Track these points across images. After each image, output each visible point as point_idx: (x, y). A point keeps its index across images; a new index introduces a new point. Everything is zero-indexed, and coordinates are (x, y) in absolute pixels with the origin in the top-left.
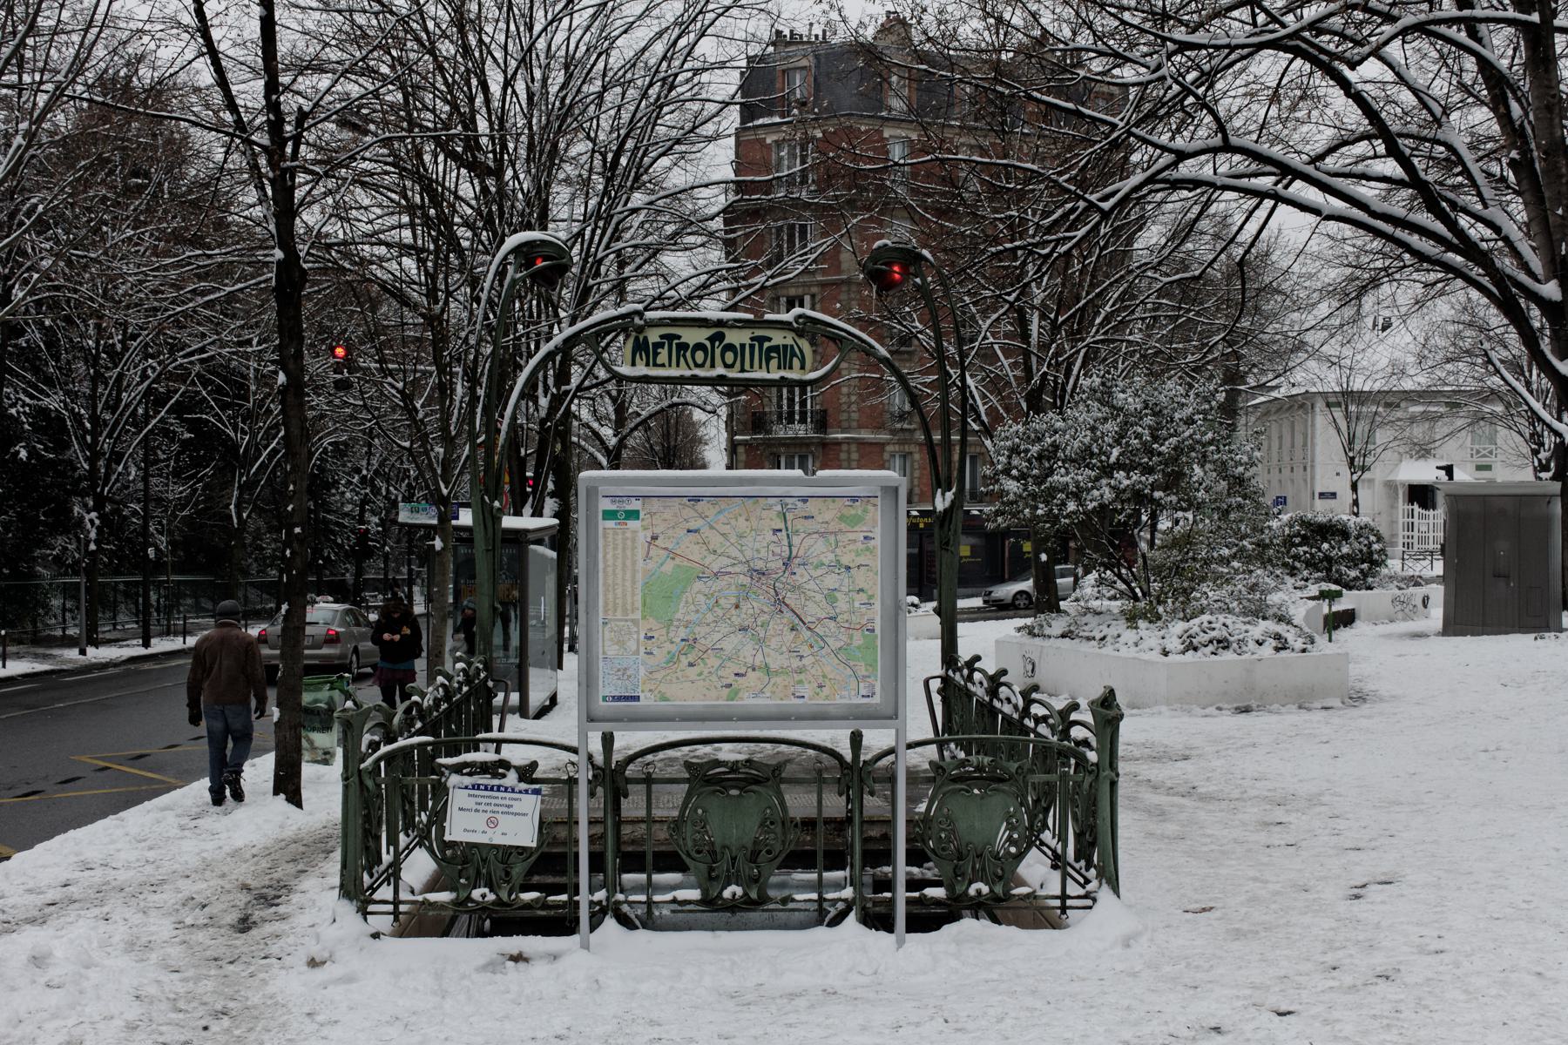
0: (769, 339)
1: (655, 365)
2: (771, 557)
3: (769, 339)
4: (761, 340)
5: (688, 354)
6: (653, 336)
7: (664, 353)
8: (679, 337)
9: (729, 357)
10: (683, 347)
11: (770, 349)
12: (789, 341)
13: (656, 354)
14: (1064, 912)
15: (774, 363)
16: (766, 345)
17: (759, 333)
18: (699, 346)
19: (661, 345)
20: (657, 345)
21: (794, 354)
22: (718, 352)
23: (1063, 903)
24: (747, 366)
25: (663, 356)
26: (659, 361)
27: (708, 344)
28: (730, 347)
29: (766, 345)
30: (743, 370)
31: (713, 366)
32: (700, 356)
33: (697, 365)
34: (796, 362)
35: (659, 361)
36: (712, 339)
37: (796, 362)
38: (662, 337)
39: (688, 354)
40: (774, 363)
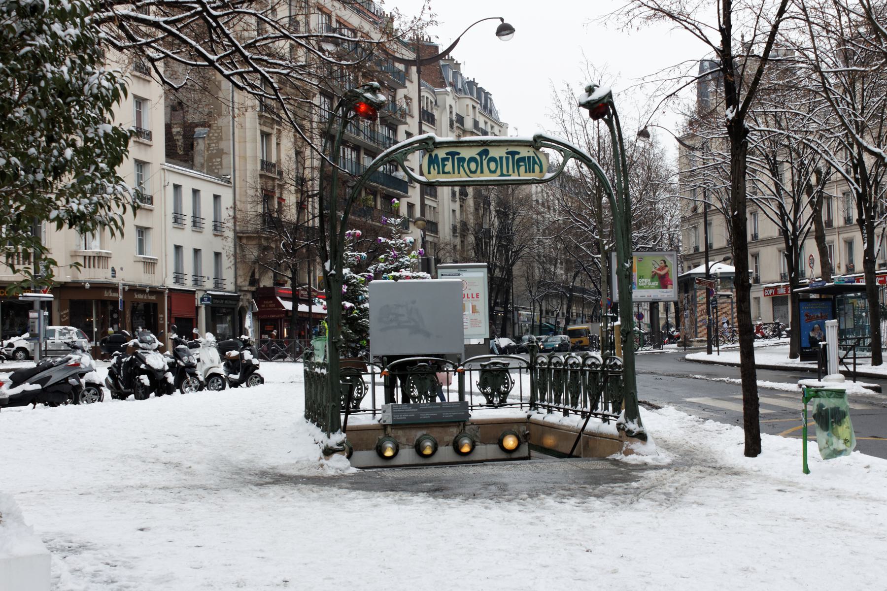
0: (518, 153)
1: (444, 173)
3: (518, 153)
4: (513, 154)
5: (465, 165)
7: (449, 164)
8: (459, 154)
9: (493, 165)
10: (462, 160)
12: (531, 154)
13: (444, 166)
15: (522, 169)
16: (517, 157)
17: (511, 149)
18: (472, 159)
19: (447, 159)
20: (444, 160)
21: (535, 163)
22: (485, 163)
24: (505, 172)
25: (449, 167)
26: (446, 170)
27: (478, 158)
28: (493, 159)
29: (517, 157)
30: (502, 175)
31: (482, 172)
32: (473, 166)
33: (471, 172)
34: (537, 168)
35: (446, 170)
36: (480, 154)
37: (537, 168)
38: (447, 154)
40: (522, 169)
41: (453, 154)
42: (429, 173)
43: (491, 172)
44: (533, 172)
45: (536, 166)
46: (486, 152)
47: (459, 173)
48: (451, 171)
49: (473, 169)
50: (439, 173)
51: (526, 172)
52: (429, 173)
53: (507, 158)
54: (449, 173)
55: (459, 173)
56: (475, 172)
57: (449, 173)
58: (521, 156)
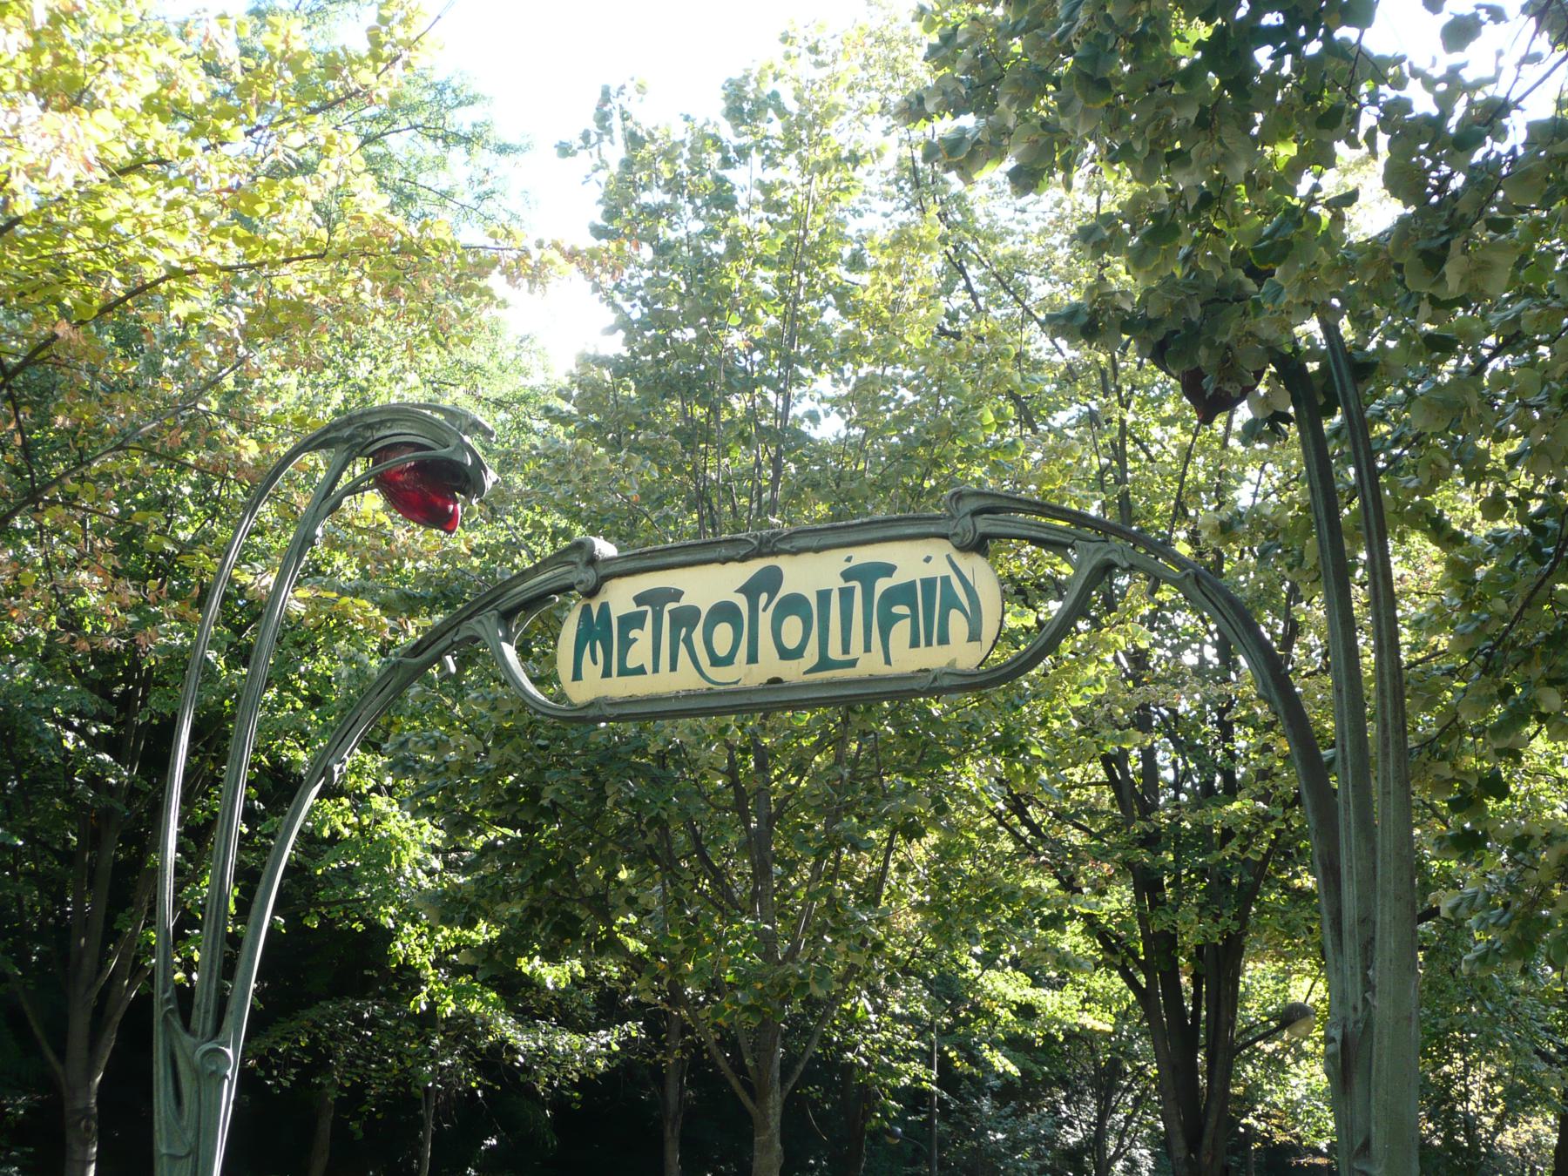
1: (624, 672)
3: (888, 570)
4: (867, 574)
5: (698, 636)
7: (642, 638)
8: (677, 595)
9: (792, 629)
10: (685, 618)
11: (891, 596)
13: (626, 644)
16: (882, 585)
18: (725, 612)
20: (631, 621)
21: (951, 602)
22: (765, 619)
24: (835, 652)
25: (640, 654)
27: (742, 602)
28: (795, 604)
29: (882, 585)
31: (752, 658)
32: (723, 635)
33: (716, 661)
34: (958, 624)
35: (631, 663)
36: (750, 590)
37: (958, 624)
38: (640, 599)
39: (698, 636)
42: (577, 676)
43: (785, 654)
44: (944, 640)
46: (771, 580)
47: (673, 668)
48: (649, 667)
49: (722, 650)
50: (607, 673)
51: (915, 643)
52: (577, 676)
53: (846, 595)
54: (640, 671)
55: (673, 668)
56: (728, 660)
57: (640, 671)
58: (897, 579)
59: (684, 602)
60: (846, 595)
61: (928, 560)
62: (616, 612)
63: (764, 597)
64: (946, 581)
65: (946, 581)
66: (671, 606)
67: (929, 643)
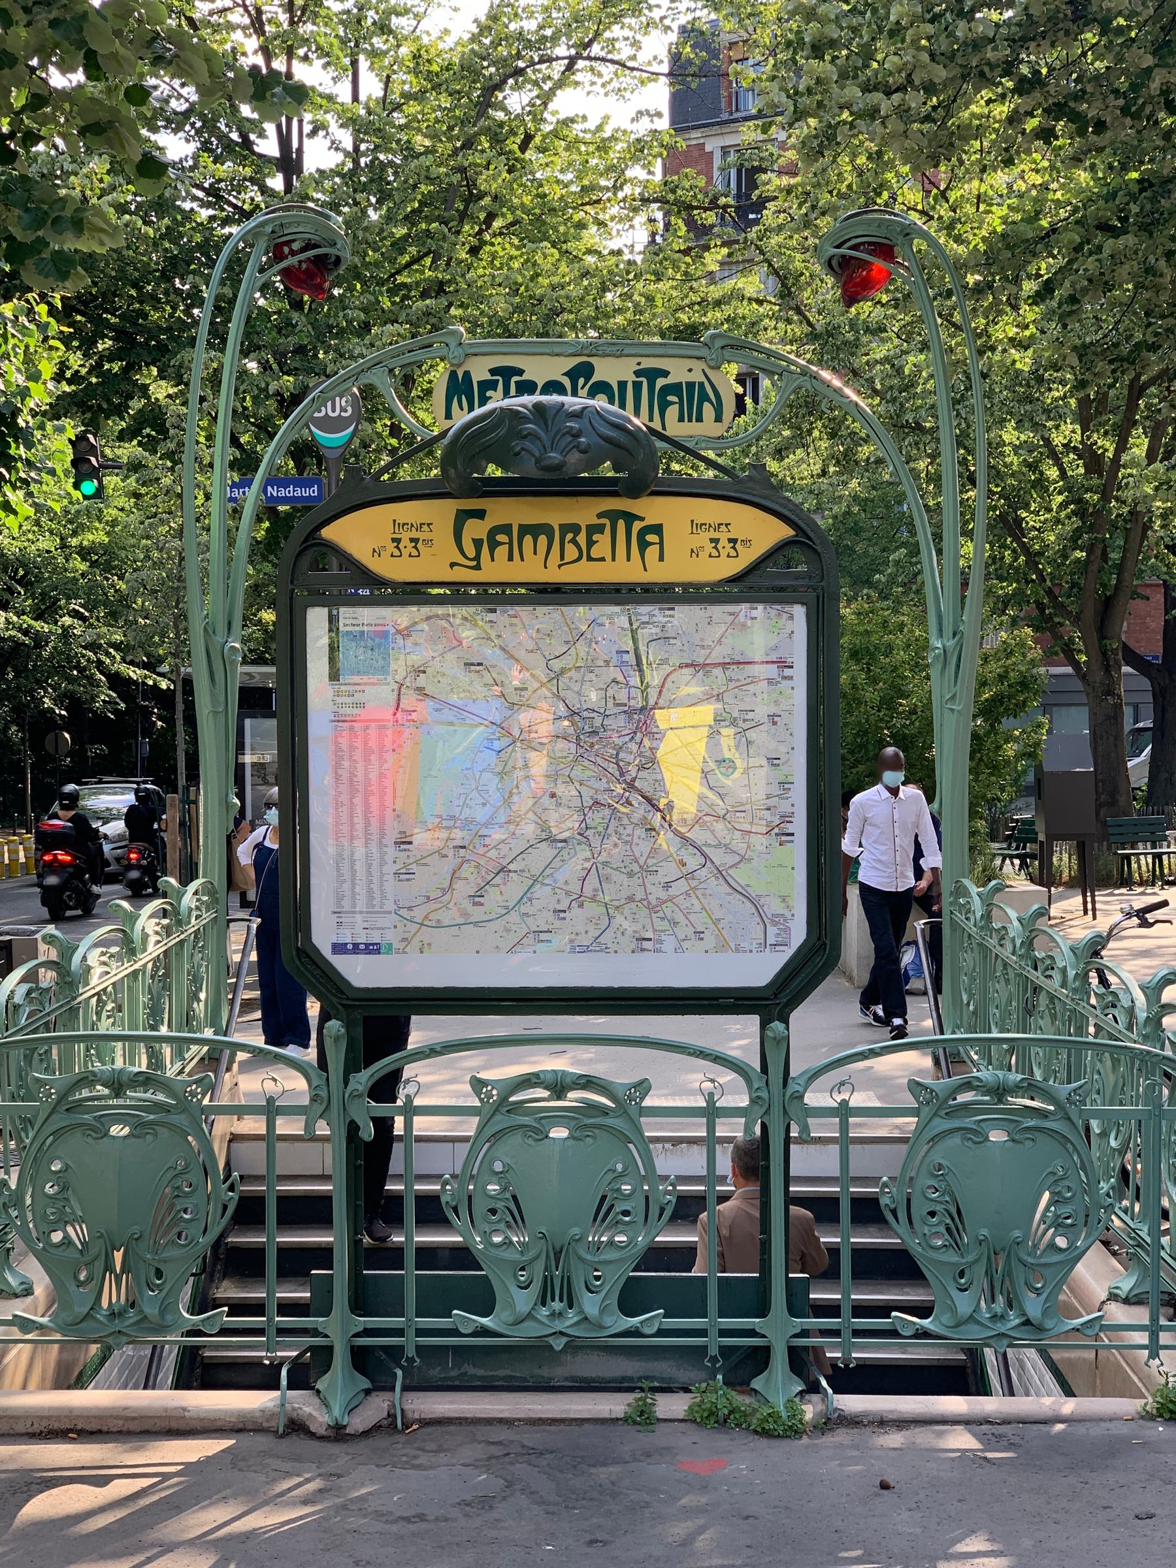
0: (665, 374)
2: (611, 709)
3: (665, 374)
4: (653, 374)
6: (480, 371)
8: (520, 372)
11: (666, 390)
14: (1154, 1355)
15: (672, 412)
16: (660, 382)
17: (648, 363)
21: (704, 397)
23: (1154, 1337)
29: (660, 382)
34: (708, 410)
36: (573, 374)
37: (708, 410)
38: (493, 372)
40: (672, 412)
41: (506, 372)
44: (700, 419)
45: (706, 405)
51: (681, 419)
53: (637, 386)
59: (525, 377)
60: (637, 386)
61: (690, 370)
62: (476, 378)
63: (581, 381)
64: (701, 384)
65: (701, 384)
66: (515, 379)
67: (690, 420)
